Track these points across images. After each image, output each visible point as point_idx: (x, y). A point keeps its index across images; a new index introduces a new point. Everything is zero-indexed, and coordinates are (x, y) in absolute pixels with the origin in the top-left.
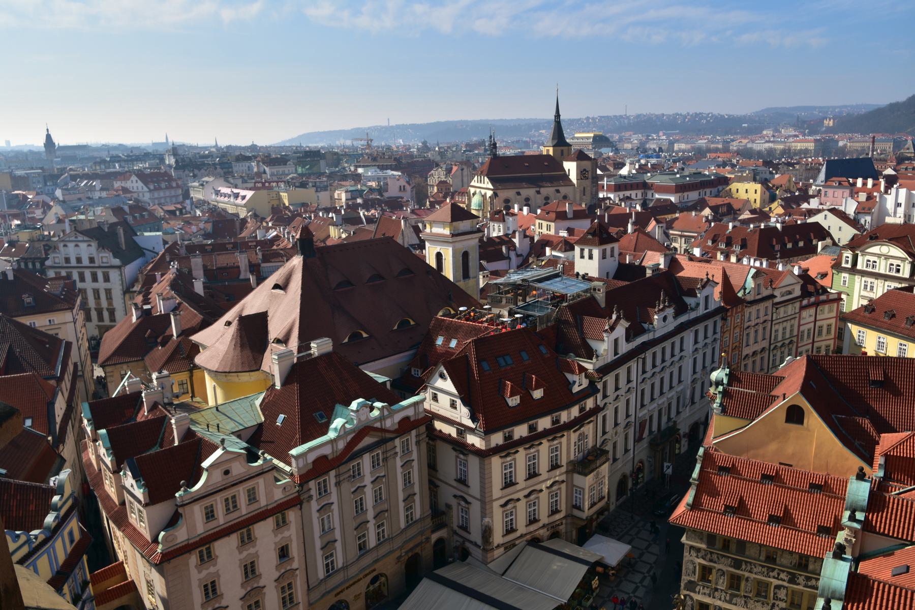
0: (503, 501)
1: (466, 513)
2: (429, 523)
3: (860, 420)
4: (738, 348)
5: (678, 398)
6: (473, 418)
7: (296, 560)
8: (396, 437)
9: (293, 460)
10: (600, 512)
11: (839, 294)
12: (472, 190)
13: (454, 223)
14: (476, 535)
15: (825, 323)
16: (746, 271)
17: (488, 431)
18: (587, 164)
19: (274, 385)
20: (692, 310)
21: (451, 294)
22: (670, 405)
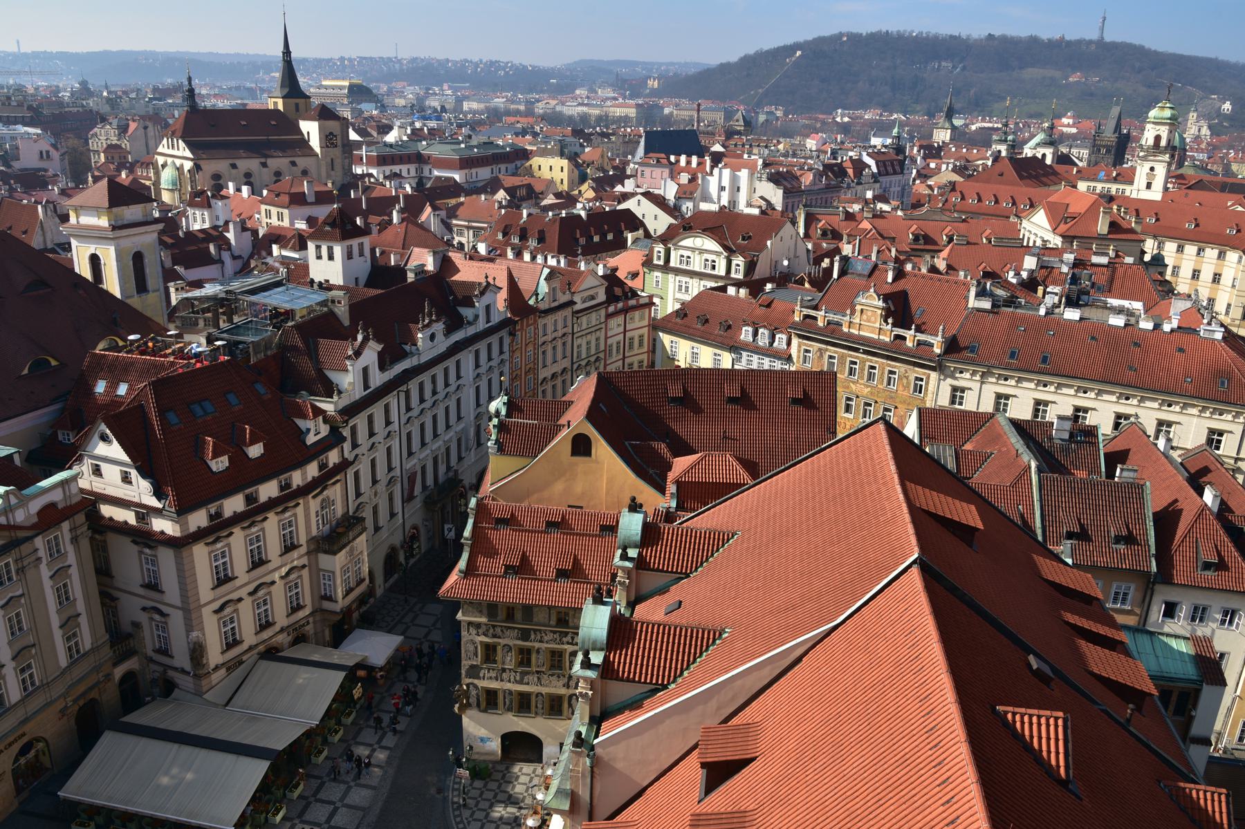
0: (217, 605)
2: (107, 653)
3: (655, 444)
4: (533, 370)
5: (459, 440)
6: (158, 494)
8: (37, 535)
10: (362, 600)
11: (651, 297)
12: (161, 160)
13: (115, 210)
14: (181, 658)
16: (537, 272)
18: (333, 125)
20: (470, 323)
21: (115, 316)
22: (448, 449)
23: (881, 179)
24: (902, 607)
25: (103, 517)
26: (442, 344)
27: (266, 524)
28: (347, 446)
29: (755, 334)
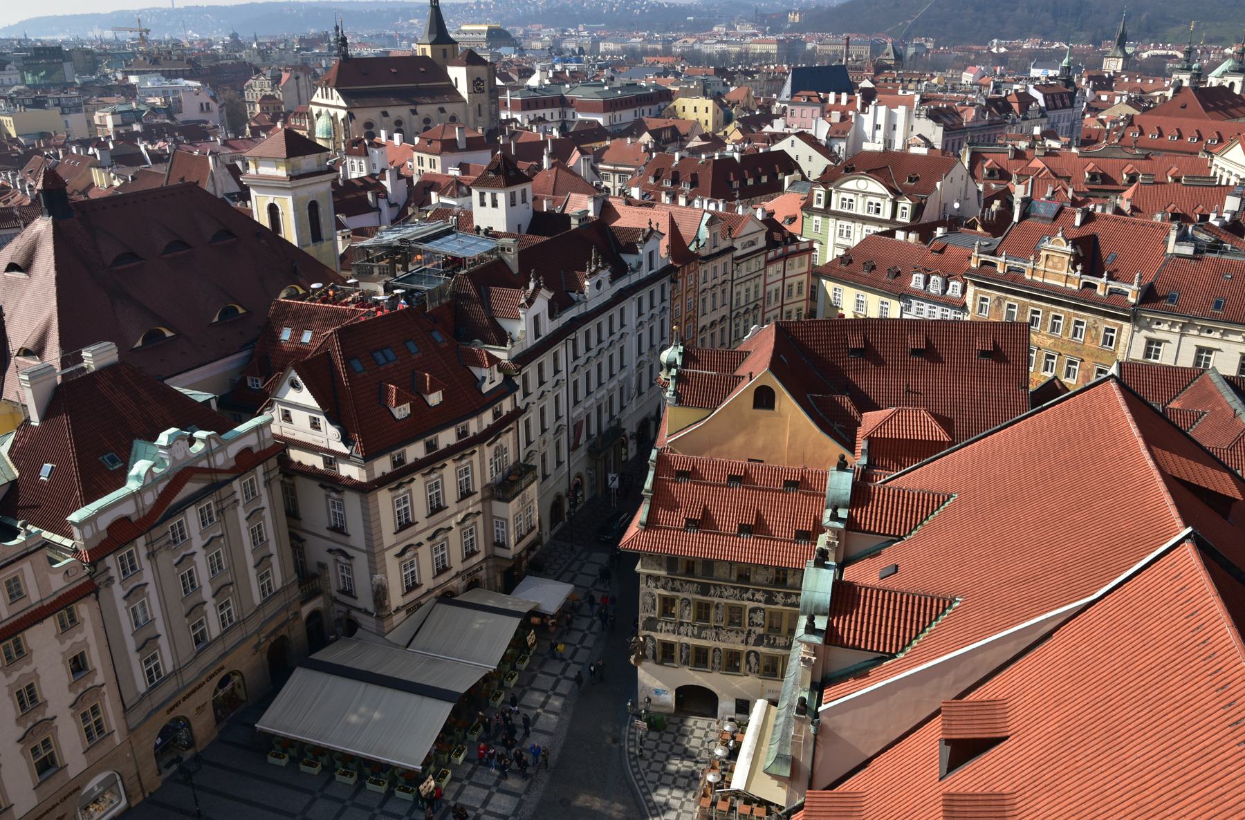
0: (398, 549)
1: (349, 572)
2: (295, 592)
3: (838, 398)
4: (693, 318)
5: (621, 389)
6: (346, 440)
7: (100, 671)
9: (75, 530)
10: (531, 547)
11: (811, 242)
12: (315, 109)
13: (292, 160)
14: (365, 600)
15: (795, 281)
16: (698, 216)
17: (369, 456)
18: (481, 71)
19: (28, 420)
20: (634, 271)
21: (296, 265)
22: (611, 398)
23: (1049, 113)
24: (1178, 585)
25: (292, 462)
26: (608, 292)
27: (444, 471)
28: (519, 394)
29: (927, 281)
